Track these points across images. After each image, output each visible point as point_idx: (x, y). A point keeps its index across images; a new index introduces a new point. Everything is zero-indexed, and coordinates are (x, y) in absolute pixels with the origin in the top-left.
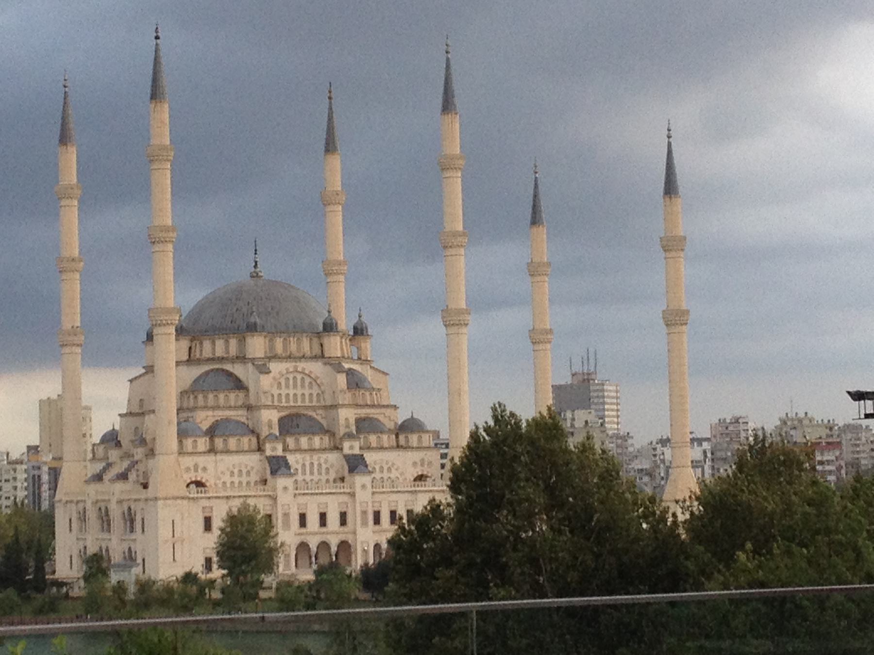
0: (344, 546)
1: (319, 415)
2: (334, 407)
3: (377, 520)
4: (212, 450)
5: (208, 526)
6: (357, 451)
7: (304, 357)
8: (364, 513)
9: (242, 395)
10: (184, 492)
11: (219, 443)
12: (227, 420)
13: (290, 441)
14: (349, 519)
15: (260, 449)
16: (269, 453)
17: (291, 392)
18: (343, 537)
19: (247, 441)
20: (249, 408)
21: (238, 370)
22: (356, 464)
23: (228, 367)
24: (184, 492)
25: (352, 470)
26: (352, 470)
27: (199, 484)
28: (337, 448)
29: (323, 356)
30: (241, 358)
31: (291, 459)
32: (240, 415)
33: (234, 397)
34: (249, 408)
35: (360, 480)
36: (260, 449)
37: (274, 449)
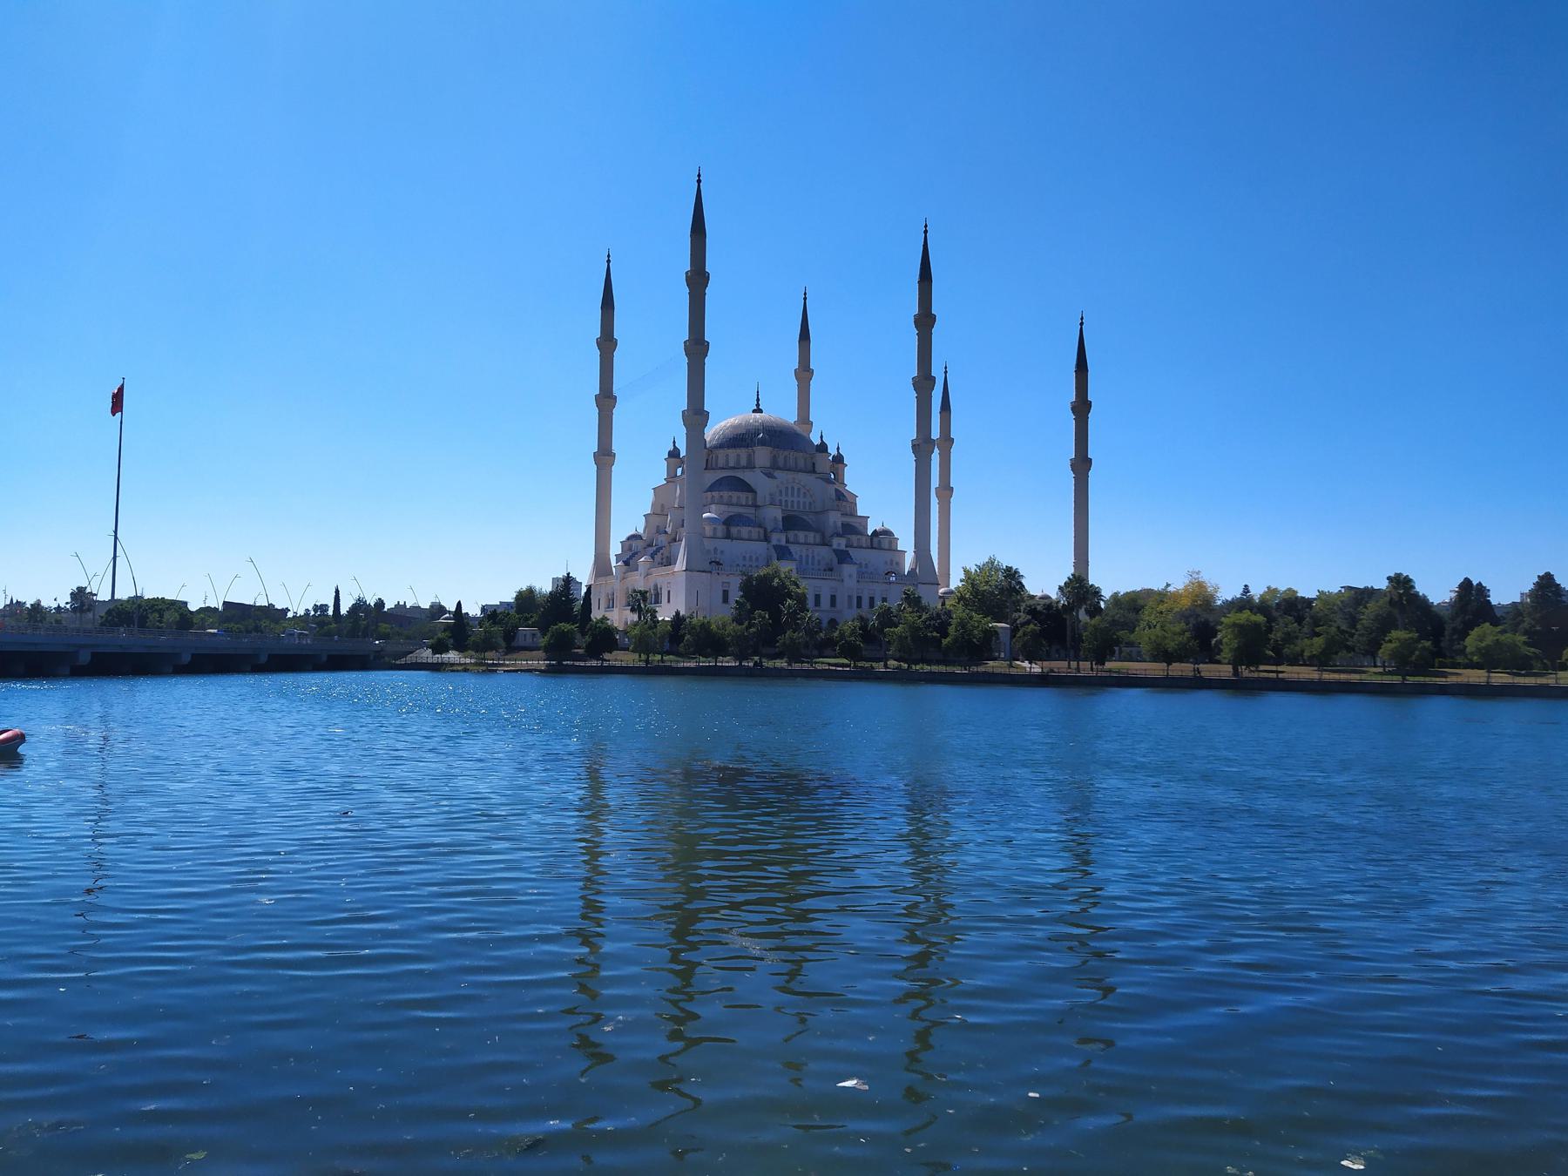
0: (833, 623)
1: (810, 519)
2: (824, 512)
3: (859, 605)
4: (728, 536)
5: (726, 600)
6: (843, 547)
7: (797, 470)
8: (850, 597)
9: (750, 495)
10: (708, 567)
11: (734, 530)
12: (740, 515)
13: (791, 534)
14: (838, 600)
15: (767, 539)
16: (774, 542)
17: (790, 499)
18: (832, 616)
19: (755, 532)
20: (756, 506)
21: (747, 476)
22: (843, 557)
23: (739, 474)
24: (708, 567)
25: (840, 562)
26: (840, 562)
27: (718, 563)
28: (825, 543)
29: (814, 471)
30: (750, 466)
31: (793, 548)
32: (749, 512)
33: (743, 497)
34: (756, 506)
35: (848, 569)
36: (767, 539)
37: (779, 538)
